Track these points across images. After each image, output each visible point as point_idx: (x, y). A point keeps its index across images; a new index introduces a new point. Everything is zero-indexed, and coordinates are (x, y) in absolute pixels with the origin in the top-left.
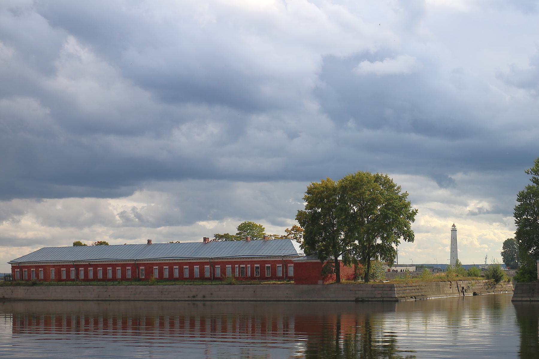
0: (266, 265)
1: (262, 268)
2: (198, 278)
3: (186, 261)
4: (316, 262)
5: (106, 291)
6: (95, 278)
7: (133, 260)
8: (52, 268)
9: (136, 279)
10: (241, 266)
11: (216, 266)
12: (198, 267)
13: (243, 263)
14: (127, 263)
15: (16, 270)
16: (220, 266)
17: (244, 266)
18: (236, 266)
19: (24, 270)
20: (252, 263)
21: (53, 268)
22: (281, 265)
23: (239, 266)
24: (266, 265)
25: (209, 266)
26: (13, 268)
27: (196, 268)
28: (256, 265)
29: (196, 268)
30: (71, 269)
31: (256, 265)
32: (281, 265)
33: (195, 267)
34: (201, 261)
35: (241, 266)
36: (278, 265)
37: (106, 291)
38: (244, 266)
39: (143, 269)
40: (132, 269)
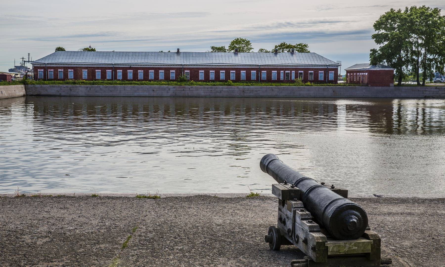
0: (309, 72)
1: (306, 74)
2: (276, 80)
3: (233, 67)
4: (389, 70)
5: (184, 90)
6: (56, 78)
7: (182, 65)
8: (84, 69)
11: (262, 72)
12: (245, 71)
13: (288, 69)
14: (171, 67)
15: (39, 70)
16: (266, 71)
17: (289, 72)
18: (281, 71)
19: (49, 70)
20: (296, 70)
21: (86, 69)
22: (323, 72)
23: (284, 72)
24: (309, 72)
25: (255, 71)
27: (243, 73)
28: (300, 72)
29: (243, 73)
30: (107, 70)
31: (300, 72)
32: (323, 72)
33: (241, 71)
36: (320, 72)
37: (184, 90)
38: (289, 72)
39: (188, 72)
40: (176, 72)
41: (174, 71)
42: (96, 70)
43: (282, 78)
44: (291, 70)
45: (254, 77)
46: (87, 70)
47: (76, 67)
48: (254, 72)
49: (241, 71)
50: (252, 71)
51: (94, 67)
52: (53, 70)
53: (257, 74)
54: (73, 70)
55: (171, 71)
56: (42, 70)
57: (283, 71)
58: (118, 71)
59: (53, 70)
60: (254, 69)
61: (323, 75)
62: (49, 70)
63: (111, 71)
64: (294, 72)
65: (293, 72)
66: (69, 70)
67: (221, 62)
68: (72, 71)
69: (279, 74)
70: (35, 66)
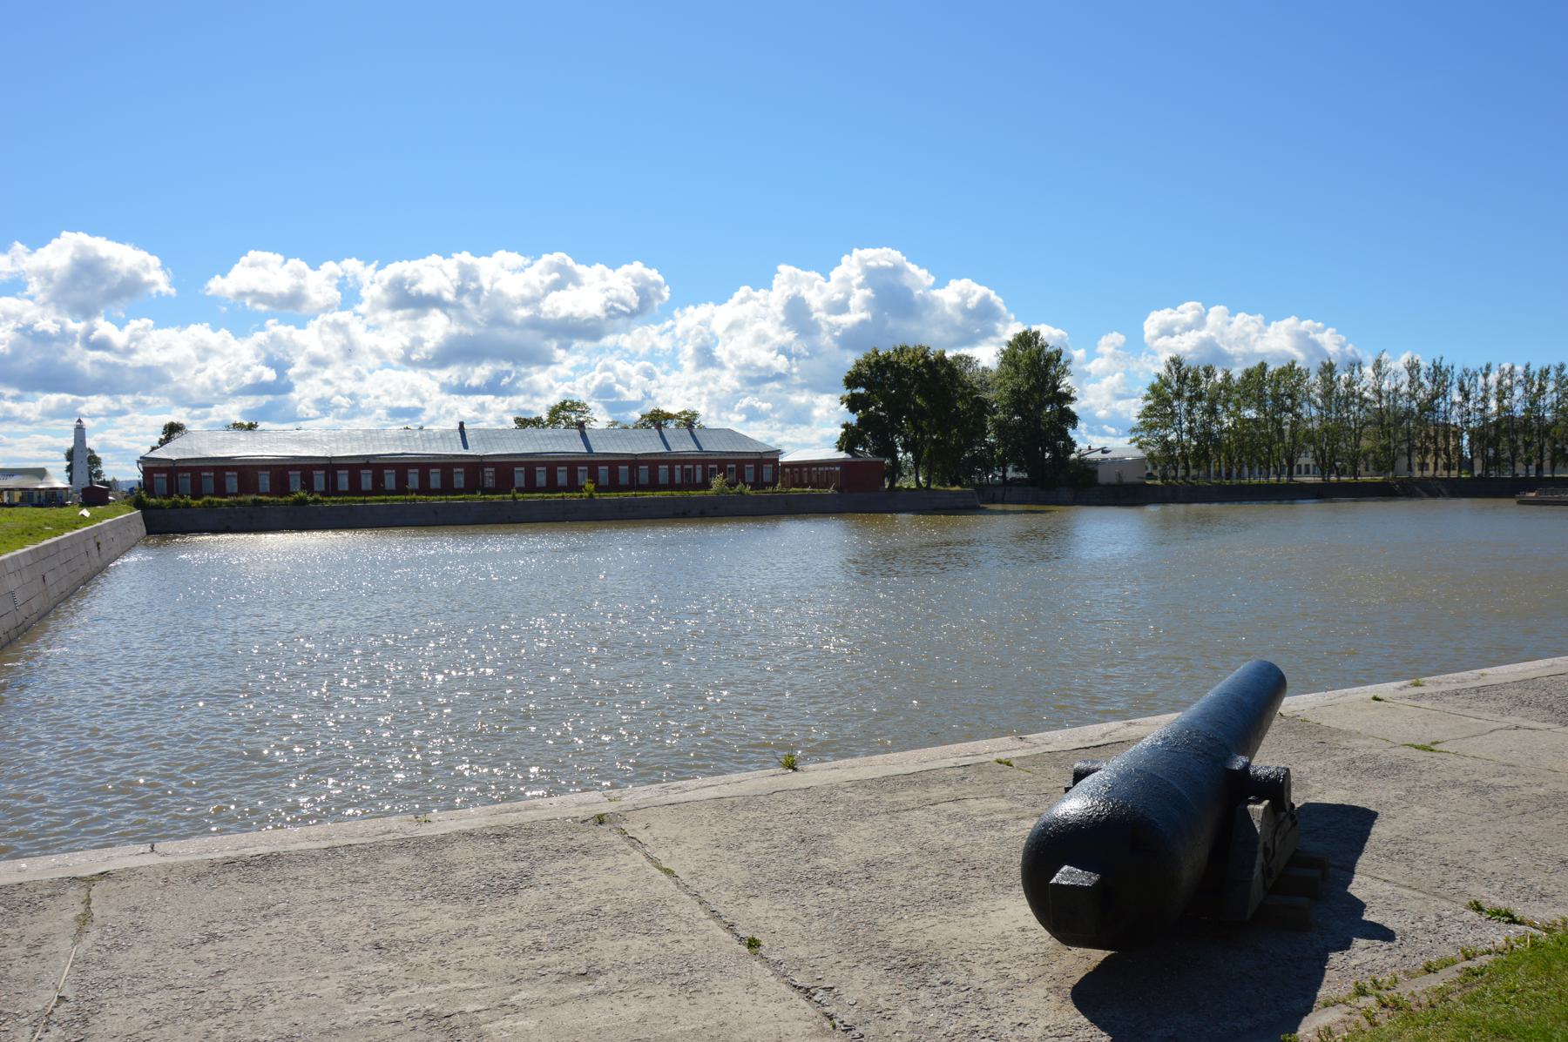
0: (729, 466)
9: (447, 488)
10: (687, 467)
11: (641, 467)
12: (607, 468)
15: (155, 475)
17: (691, 467)
19: (180, 475)
23: (682, 468)
24: (729, 466)
25: (627, 467)
26: (147, 472)
28: (711, 466)
31: (711, 466)
33: (600, 468)
34: (613, 459)
35: (687, 467)
38: (691, 467)
41: (462, 470)
42: (290, 473)
43: (678, 479)
44: (695, 462)
45: (624, 479)
46: (268, 473)
47: (244, 466)
48: (623, 468)
49: (600, 468)
50: (620, 467)
51: (284, 466)
52: (189, 474)
53: (631, 471)
54: (235, 474)
55: (455, 470)
56: (164, 475)
57: (679, 466)
58: (339, 472)
59: (189, 474)
60: (623, 463)
61: (752, 471)
62: (180, 475)
63: (323, 472)
64: (700, 466)
65: (699, 466)
66: (227, 473)
67: (557, 449)
68: (234, 476)
69: (672, 472)
70: (147, 465)
